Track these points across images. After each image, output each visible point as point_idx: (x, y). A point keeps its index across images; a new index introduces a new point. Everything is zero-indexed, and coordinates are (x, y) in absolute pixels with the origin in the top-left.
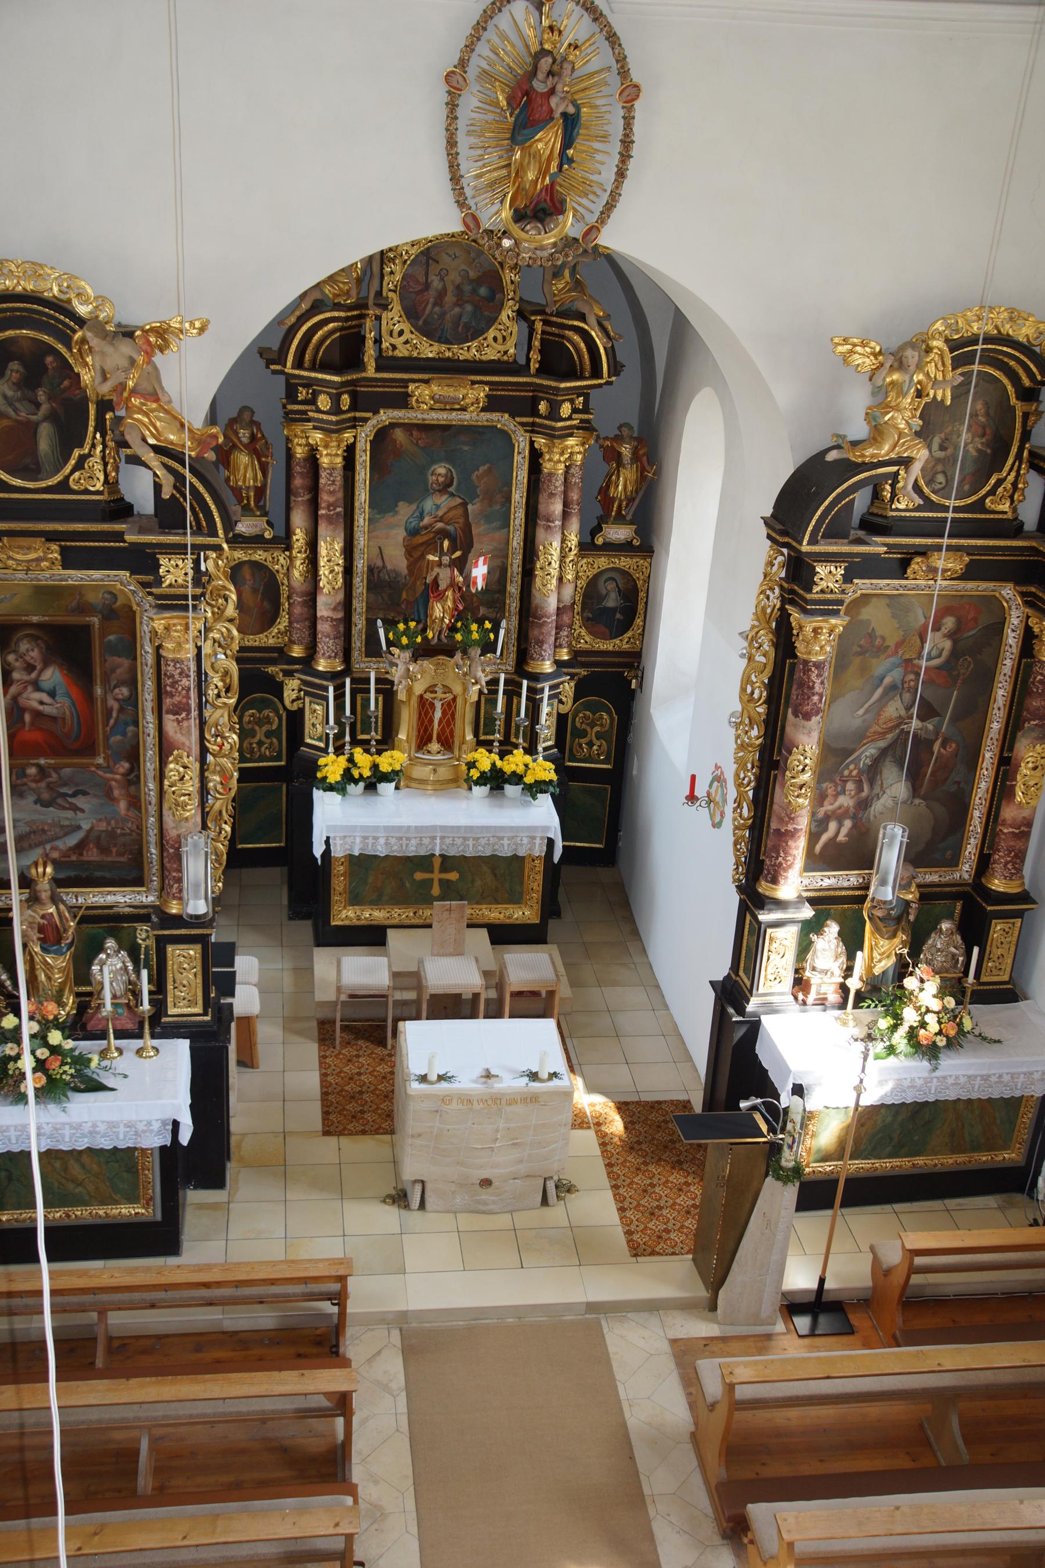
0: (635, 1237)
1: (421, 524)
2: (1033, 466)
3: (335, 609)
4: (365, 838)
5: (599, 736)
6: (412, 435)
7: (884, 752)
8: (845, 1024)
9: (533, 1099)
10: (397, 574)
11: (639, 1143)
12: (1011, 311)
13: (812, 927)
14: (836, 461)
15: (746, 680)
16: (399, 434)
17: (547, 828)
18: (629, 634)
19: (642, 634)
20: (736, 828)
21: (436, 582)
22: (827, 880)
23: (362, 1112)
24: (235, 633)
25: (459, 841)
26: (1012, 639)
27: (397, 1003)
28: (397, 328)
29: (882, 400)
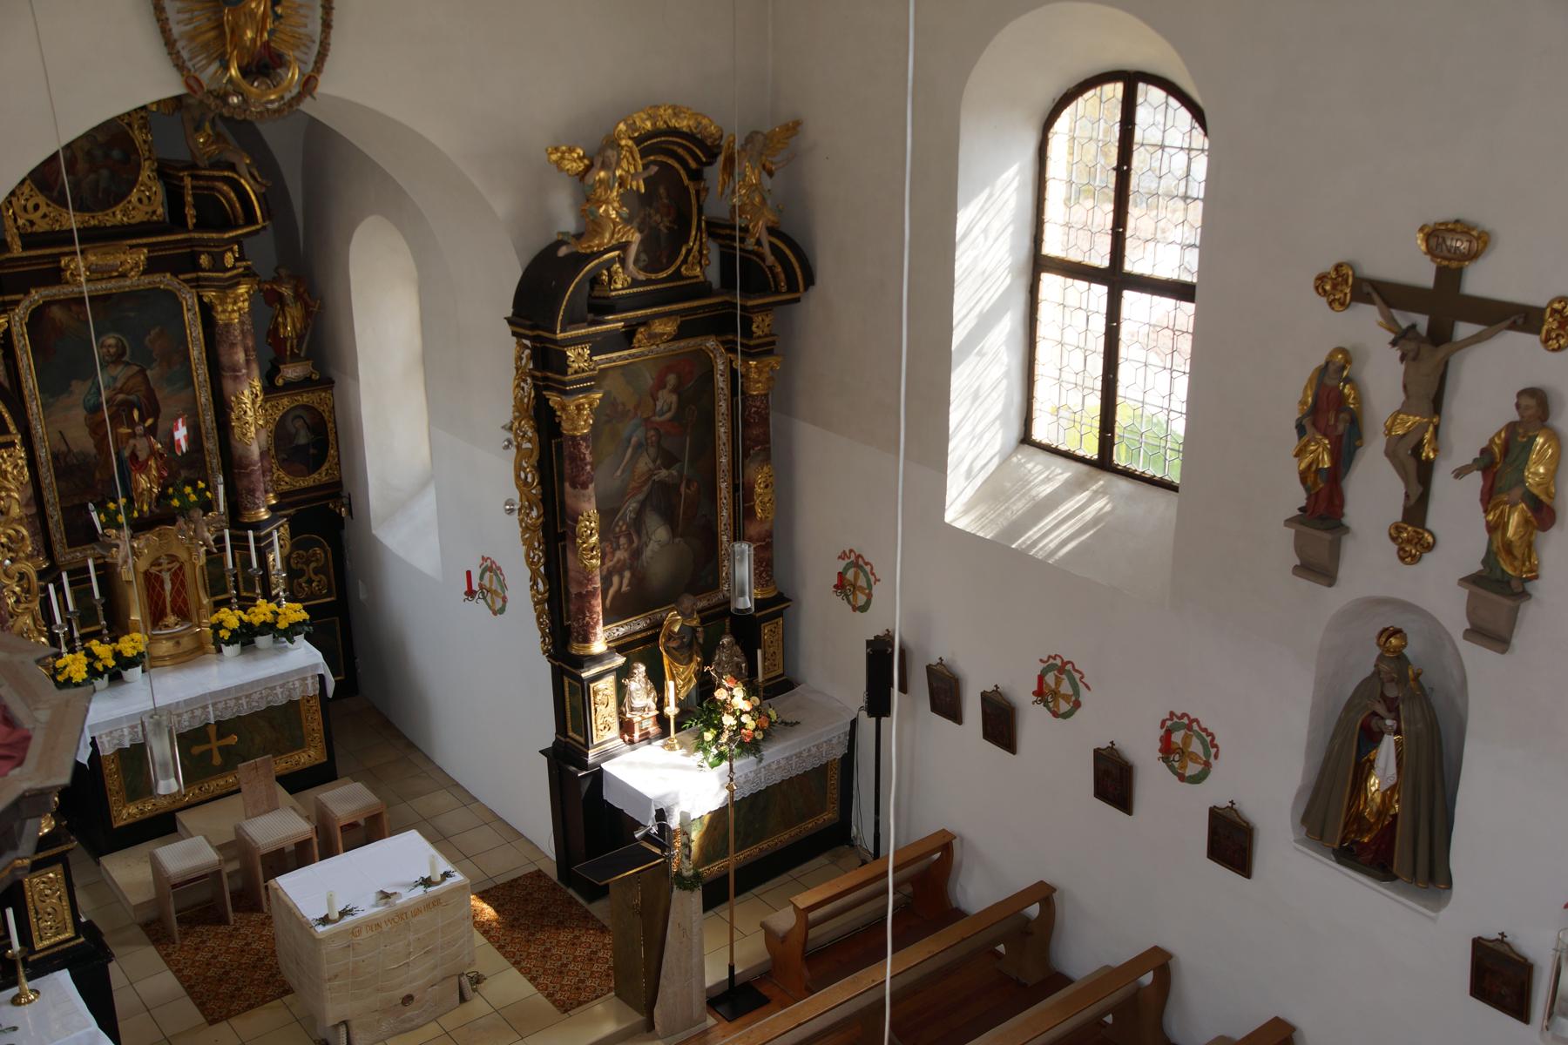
0: (557, 996)
2: (711, 235)
3: (27, 505)
7: (643, 504)
8: (672, 748)
9: (435, 902)
11: (516, 920)
12: (674, 107)
13: (624, 673)
14: (567, 256)
15: (518, 468)
16: (56, 312)
17: (316, 666)
18: (326, 466)
19: (339, 463)
20: (536, 604)
21: (134, 456)
22: (620, 630)
23: (239, 989)
24: (25, 532)
25: (232, 703)
26: (721, 382)
27: (230, 875)
28: (30, 205)
29: (587, 199)
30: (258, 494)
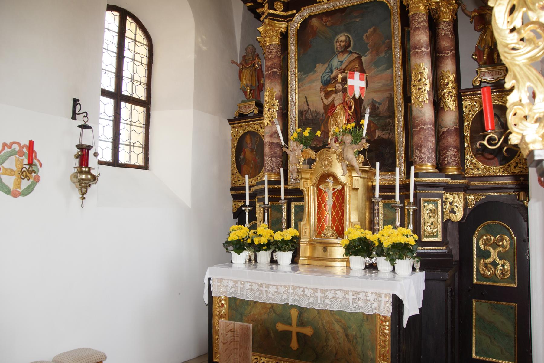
1: (332, 76)
4: (236, 282)
5: (501, 256)
6: (322, 20)
10: (317, 113)
16: (315, 22)
30: (424, 150)
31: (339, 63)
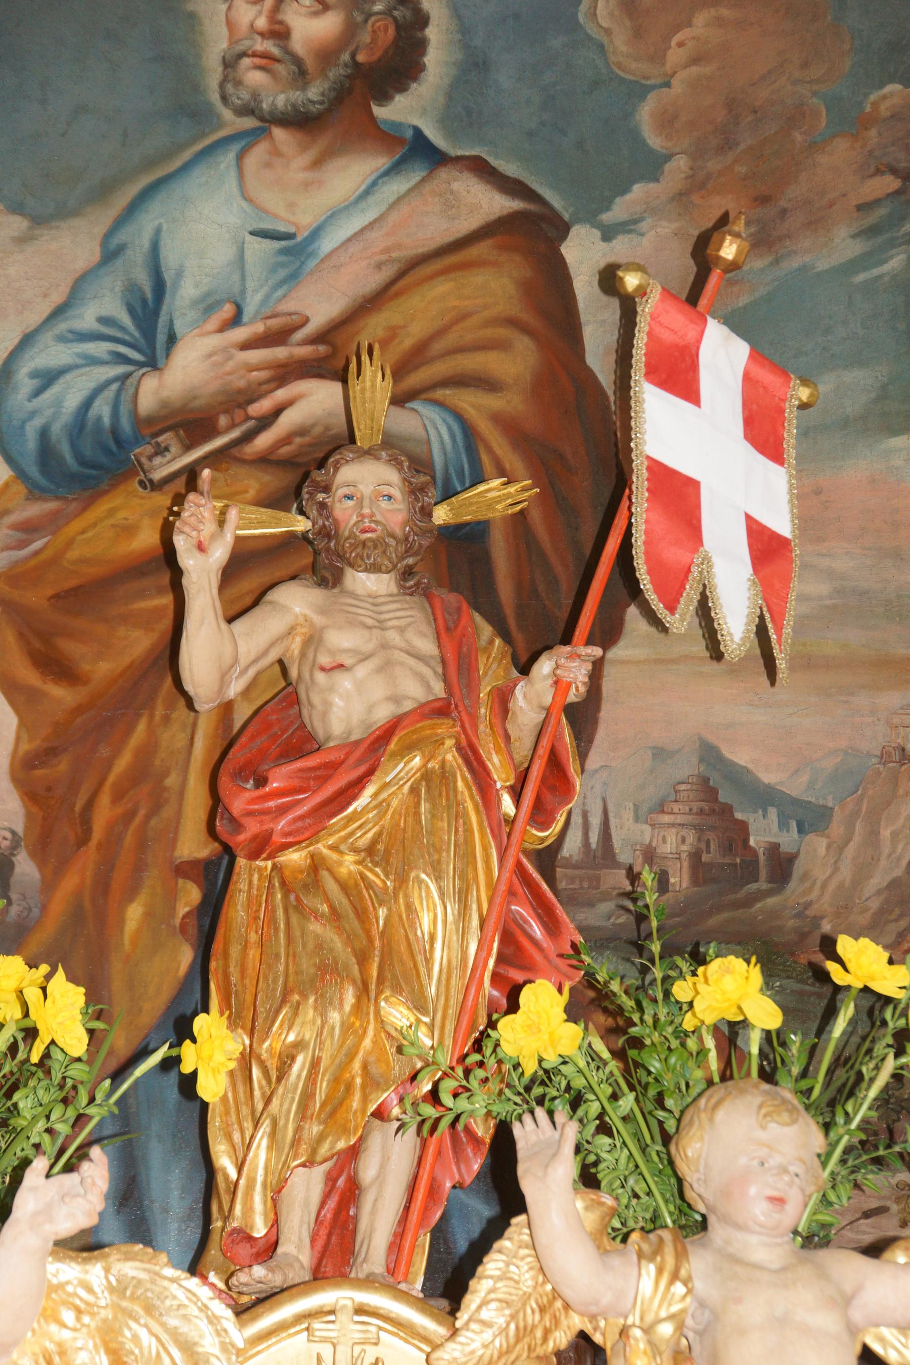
1: (153, 392)
31: (259, 251)
